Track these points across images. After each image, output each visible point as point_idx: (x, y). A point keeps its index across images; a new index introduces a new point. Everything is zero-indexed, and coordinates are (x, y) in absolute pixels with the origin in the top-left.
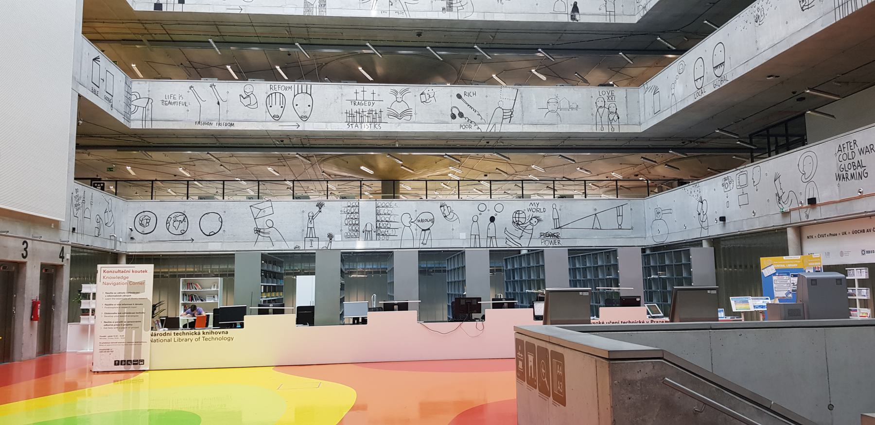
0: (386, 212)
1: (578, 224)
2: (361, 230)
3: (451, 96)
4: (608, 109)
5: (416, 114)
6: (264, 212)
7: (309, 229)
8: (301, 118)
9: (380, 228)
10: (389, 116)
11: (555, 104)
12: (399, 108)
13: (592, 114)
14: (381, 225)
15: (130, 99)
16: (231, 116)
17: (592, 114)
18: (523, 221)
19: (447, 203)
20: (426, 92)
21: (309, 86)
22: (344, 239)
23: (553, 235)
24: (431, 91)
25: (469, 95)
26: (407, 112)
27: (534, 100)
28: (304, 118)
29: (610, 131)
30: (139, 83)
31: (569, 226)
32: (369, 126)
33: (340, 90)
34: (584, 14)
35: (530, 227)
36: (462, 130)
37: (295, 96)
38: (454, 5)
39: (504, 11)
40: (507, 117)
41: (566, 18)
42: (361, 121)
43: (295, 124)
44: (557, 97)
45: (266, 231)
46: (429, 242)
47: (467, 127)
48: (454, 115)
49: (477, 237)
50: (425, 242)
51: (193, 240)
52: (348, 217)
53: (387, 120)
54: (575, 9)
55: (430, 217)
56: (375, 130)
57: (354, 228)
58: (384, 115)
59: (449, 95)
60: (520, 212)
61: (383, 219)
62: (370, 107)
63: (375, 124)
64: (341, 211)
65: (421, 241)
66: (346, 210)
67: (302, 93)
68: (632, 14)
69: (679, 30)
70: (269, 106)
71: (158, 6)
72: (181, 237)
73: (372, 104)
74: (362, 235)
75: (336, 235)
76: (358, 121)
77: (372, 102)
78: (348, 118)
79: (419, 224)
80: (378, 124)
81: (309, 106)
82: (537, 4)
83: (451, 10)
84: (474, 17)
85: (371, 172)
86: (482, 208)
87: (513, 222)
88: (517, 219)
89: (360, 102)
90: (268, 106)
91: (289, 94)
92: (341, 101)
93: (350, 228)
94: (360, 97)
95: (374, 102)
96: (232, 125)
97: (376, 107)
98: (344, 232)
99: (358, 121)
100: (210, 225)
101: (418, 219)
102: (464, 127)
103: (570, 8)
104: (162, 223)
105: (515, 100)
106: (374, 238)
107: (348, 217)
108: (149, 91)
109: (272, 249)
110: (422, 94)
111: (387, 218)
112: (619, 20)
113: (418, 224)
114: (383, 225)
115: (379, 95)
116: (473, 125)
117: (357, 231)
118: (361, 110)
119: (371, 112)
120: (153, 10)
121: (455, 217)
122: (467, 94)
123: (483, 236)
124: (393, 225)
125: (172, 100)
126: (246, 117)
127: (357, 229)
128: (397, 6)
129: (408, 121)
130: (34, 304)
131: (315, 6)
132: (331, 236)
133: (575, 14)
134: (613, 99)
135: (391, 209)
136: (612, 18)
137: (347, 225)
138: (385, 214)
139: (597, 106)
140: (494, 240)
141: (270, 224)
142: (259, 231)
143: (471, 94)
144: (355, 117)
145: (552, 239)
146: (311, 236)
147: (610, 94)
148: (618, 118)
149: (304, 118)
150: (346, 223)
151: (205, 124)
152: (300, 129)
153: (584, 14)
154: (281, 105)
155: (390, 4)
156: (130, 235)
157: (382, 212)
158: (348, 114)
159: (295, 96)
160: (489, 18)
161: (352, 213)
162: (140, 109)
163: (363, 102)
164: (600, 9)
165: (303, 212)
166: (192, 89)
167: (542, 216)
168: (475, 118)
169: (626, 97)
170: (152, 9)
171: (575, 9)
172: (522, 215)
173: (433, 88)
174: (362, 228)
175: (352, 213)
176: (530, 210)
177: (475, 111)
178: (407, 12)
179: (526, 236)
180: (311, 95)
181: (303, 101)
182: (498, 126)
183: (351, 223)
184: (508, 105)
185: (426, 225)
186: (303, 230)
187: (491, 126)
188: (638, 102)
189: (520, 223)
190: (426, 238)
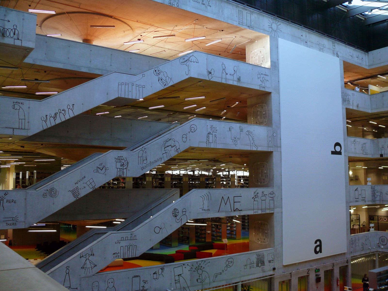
15: (374, 193)
71: (381, 155)
130: (338, 280)
162: (378, 196)
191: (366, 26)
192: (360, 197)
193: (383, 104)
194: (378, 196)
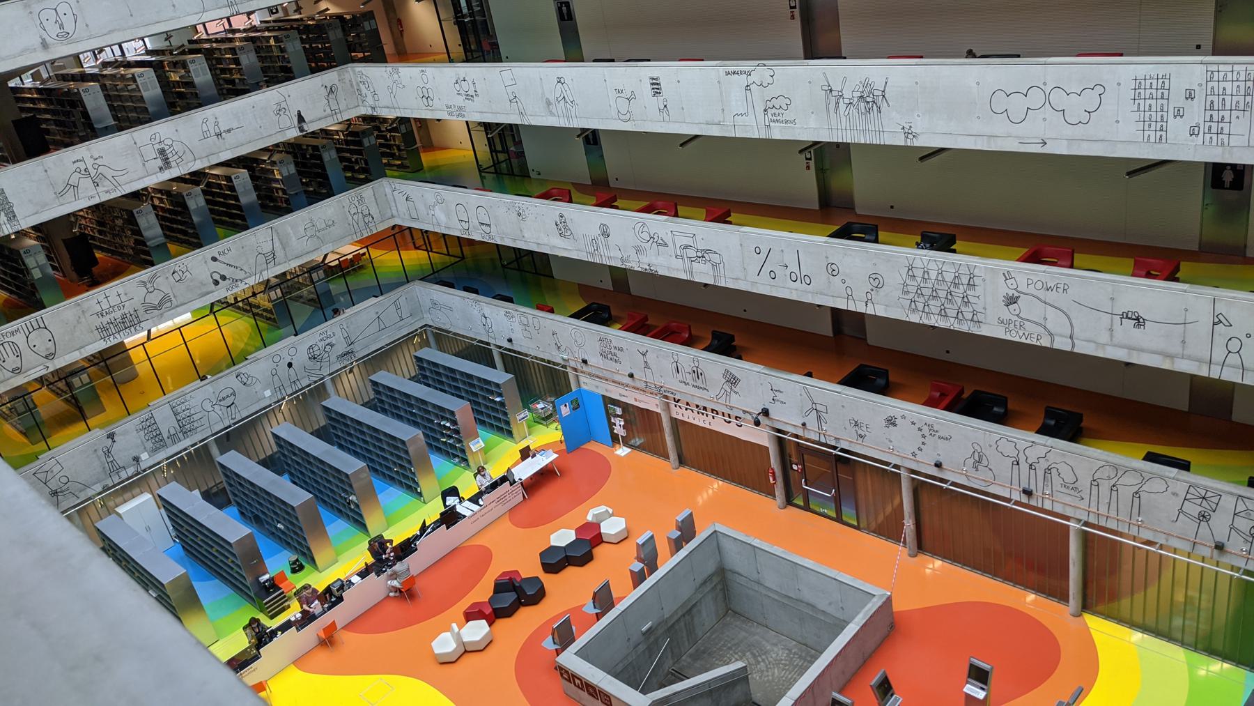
0: (183, 408)
2: (165, 437)
3: (206, 262)
6: (52, 472)
8: (46, 357)
9: (184, 426)
12: (155, 299)
13: (349, 224)
17: (349, 224)
19: (241, 370)
20: (177, 269)
22: (152, 454)
23: (348, 353)
24: (182, 266)
27: (291, 232)
28: (51, 356)
33: (78, 308)
34: (312, 122)
35: (326, 355)
37: (27, 338)
39: (228, 147)
45: (63, 488)
48: (216, 281)
49: (281, 387)
50: (234, 416)
52: (146, 432)
53: (147, 316)
54: (301, 119)
57: (157, 440)
58: (141, 313)
59: (203, 262)
61: (183, 416)
62: (122, 311)
64: (137, 430)
65: (230, 418)
66: (141, 427)
67: (34, 330)
68: (356, 104)
73: (122, 308)
74: (169, 442)
75: (141, 455)
76: (114, 332)
77: (121, 306)
79: (221, 403)
81: (50, 340)
82: (260, 127)
83: (170, 167)
87: (310, 358)
89: (107, 311)
91: (20, 339)
92: (86, 319)
93: (153, 441)
97: (128, 308)
99: (114, 332)
102: (231, 289)
103: (296, 120)
110: (173, 273)
116: (239, 283)
117: (161, 440)
118: (113, 319)
121: (254, 380)
123: (286, 384)
127: (161, 438)
132: (137, 459)
133: (303, 124)
135: (188, 403)
137: (148, 440)
138: (184, 411)
140: (298, 383)
141: (64, 480)
143: (226, 252)
144: (109, 330)
145: (348, 357)
146: (115, 469)
149: (51, 356)
150: (147, 438)
153: (312, 122)
154: (16, 354)
155: (96, 185)
157: (179, 411)
159: (27, 338)
161: (150, 426)
163: (111, 309)
164: (325, 111)
165: (95, 450)
167: (333, 340)
168: (241, 275)
169: (374, 195)
171: (301, 119)
172: (316, 348)
174: (165, 436)
175: (150, 426)
178: (119, 188)
180: (46, 328)
183: (152, 436)
184: (267, 248)
186: (104, 468)
187: (258, 276)
188: (386, 195)
189: (316, 356)
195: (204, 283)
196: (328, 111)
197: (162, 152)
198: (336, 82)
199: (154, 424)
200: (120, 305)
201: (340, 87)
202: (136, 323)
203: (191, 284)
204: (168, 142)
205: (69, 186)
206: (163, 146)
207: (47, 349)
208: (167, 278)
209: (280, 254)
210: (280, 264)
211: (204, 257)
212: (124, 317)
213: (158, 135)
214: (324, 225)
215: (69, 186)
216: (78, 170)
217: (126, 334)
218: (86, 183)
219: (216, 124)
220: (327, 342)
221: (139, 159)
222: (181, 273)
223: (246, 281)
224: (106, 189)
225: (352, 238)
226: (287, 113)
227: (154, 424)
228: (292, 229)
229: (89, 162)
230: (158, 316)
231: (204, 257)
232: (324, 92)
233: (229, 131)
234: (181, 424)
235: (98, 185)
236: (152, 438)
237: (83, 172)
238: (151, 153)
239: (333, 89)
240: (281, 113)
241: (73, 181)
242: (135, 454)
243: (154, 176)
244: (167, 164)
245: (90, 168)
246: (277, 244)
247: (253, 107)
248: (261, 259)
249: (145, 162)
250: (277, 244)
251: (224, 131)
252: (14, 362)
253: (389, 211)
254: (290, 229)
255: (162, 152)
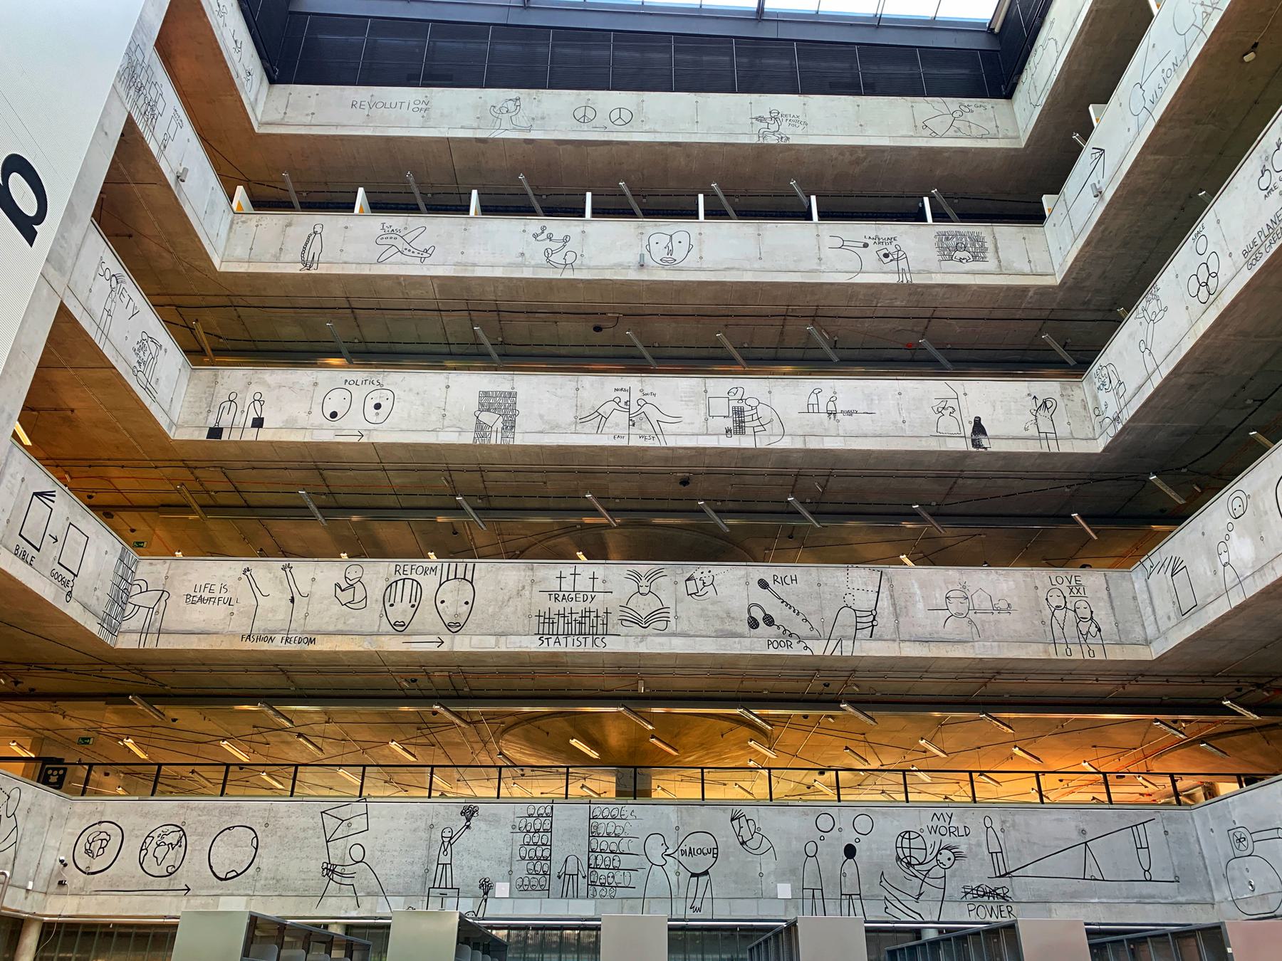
0: (610, 829)
1: (1048, 866)
2: (554, 872)
4: (1075, 611)
5: (676, 617)
6: (349, 825)
7: (440, 867)
8: (448, 626)
10: (624, 623)
11: (962, 600)
12: (644, 606)
14: (599, 862)
16: (313, 625)
18: (919, 855)
19: (745, 810)
20: (697, 575)
21: (470, 566)
23: (993, 893)
24: (706, 573)
25: (783, 581)
26: (660, 614)
27: (918, 592)
28: (455, 627)
29: (1087, 657)
30: (151, 564)
31: (1029, 870)
32: (583, 641)
36: (771, 651)
37: (440, 585)
38: (747, 424)
39: (841, 433)
40: (866, 625)
41: (963, 445)
42: (566, 633)
43: (434, 638)
44: (964, 587)
45: (348, 870)
46: (707, 905)
47: (782, 644)
49: (818, 894)
51: (189, 890)
52: (527, 839)
54: (978, 428)
55: (708, 842)
56: (595, 649)
57: (538, 868)
58: (613, 619)
59: (743, 581)
60: (913, 835)
61: (604, 846)
62: (587, 604)
63: (595, 637)
64: (514, 827)
65: (690, 902)
66: (523, 825)
67: (455, 578)
69: (1184, 467)
70: (387, 605)
72: (164, 883)
73: (590, 599)
74: (556, 885)
76: (561, 632)
77: (589, 596)
78: (541, 625)
79: (683, 859)
80: (601, 637)
81: (467, 603)
82: (904, 422)
83: (743, 433)
84: (785, 443)
85: (594, 755)
86: (825, 823)
87: (898, 858)
88: (907, 852)
90: (387, 601)
92: (531, 593)
94: (567, 585)
95: (593, 594)
96: (311, 641)
97: (599, 603)
98: (516, 876)
99: (561, 632)
100: (229, 854)
101: (682, 847)
103: (969, 429)
104: (133, 846)
105: (878, 592)
106: (583, 893)
107: (527, 839)
108: (167, 578)
109: (354, 914)
110: (688, 579)
111: (612, 843)
112: (1066, 448)
113: (682, 859)
114: (604, 861)
115: (604, 582)
117: (545, 874)
119: (587, 614)
120: (205, 439)
121: (765, 844)
122: (779, 580)
124: (626, 861)
125: (206, 595)
126: (340, 627)
127: (546, 868)
128: (644, 427)
129: (662, 633)
131: (494, 429)
132: (486, 887)
133: (980, 437)
134: (1081, 591)
135: (622, 823)
136: (1053, 443)
137: (523, 859)
138: (609, 836)
139: (1050, 606)
141: (357, 853)
142: (333, 871)
144: (555, 625)
145: (992, 903)
146: (443, 885)
147: (1073, 583)
148: (1099, 630)
149: (455, 627)
151: (259, 639)
152: (444, 648)
154: (413, 602)
155: (631, 423)
156: (59, 874)
157: (601, 831)
158: (542, 619)
159: (440, 585)
160: (814, 444)
161: (537, 831)
162: (143, 611)
163: (573, 595)
164: (1026, 429)
165: (432, 827)
166: (248, 573)
170: (203, 435)
171: (978, 428)
173: (711, 568)
174: (556, 868)
175: (537, 831)
176: (934, 830)
177: (798, 614)
179: (932, 892)
180: (471, 583)
181: (454, 596)
182: (847, 644)
183: (532, 854)
184: (864, 601)
185: (700, 863)
186: (427, 870)
187: (833, 643)
188: (1135, 598)
190: (700, 895)
191: (291, 13)
192: (51, 551)
193: (281, 249)
194: (143, 611)
195: (732, 615)
196: (1033, 431)
197: (739, 412)
198: (1057, 397)
199: (545, 831)
200: (589, 594)
201: (1061, 404)
202: (600, 632)
203: (710, 607)
204: (754, 403)
205: (596, 414)
206: (743, 405)
207: (457, 615)
208: (676, 583)
209: (885, 620)
210: (881, 639)
211: (747, 575)
212: (586, 614)
213: (740, 391)
214: (987, 605)
215: (596, 414)
216: (617, 400)
217: (577, 643)
218: (620, 418)
219: (833, 400)
220: (947, 840)
221: (703, 411)
222: (700, 584)
223: (809, 643)
224: (642, 432)
225: (1046, 651)
226: (956, 414)
227: (545, 831)
228: (921, 588)
229: (636, 395)
230: (637, 636)
231: (747, 575)
232: (1031, 405)
233: (850, 413)
234: (592, 861)
235: (634, 425)
236: (531, 859)
237: (622, 404)
238: (721, 407)
239: (1049, 404)
240: (946, 412)
241: (605, 410)
242: (487, 875)
243: (715, 437)
244: (740, 428)
245: (633, 402)
246: (885, 603)
247: (900, 394)
248: (847, 617)
249: (709, 415)
250: (885, 603)
251: (842, 412)
252: (404, 611)
253: (1138, 629)
254: (916, 586)
255: (739, 412)
